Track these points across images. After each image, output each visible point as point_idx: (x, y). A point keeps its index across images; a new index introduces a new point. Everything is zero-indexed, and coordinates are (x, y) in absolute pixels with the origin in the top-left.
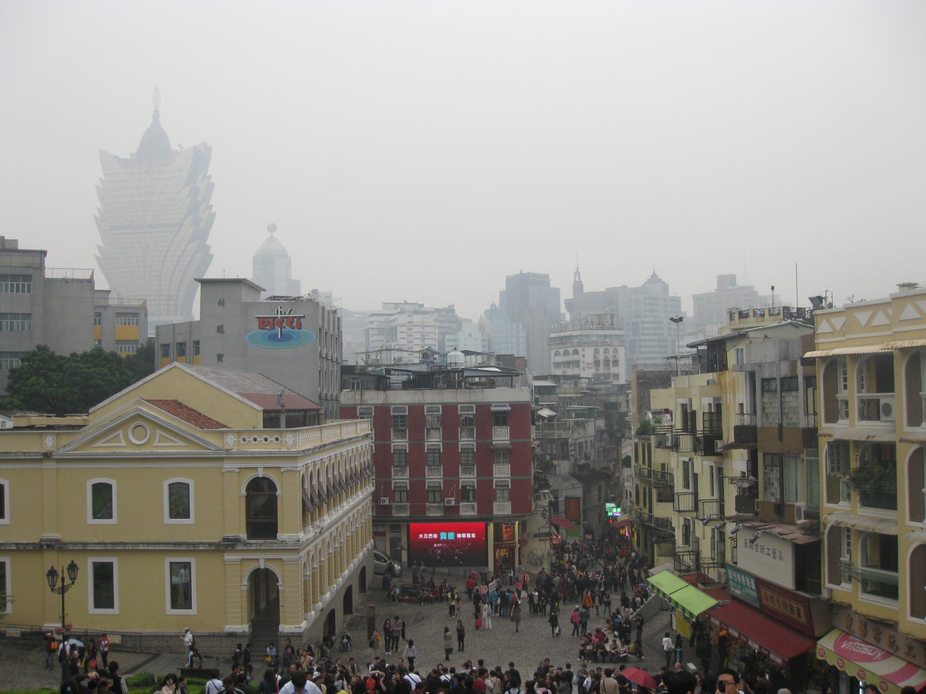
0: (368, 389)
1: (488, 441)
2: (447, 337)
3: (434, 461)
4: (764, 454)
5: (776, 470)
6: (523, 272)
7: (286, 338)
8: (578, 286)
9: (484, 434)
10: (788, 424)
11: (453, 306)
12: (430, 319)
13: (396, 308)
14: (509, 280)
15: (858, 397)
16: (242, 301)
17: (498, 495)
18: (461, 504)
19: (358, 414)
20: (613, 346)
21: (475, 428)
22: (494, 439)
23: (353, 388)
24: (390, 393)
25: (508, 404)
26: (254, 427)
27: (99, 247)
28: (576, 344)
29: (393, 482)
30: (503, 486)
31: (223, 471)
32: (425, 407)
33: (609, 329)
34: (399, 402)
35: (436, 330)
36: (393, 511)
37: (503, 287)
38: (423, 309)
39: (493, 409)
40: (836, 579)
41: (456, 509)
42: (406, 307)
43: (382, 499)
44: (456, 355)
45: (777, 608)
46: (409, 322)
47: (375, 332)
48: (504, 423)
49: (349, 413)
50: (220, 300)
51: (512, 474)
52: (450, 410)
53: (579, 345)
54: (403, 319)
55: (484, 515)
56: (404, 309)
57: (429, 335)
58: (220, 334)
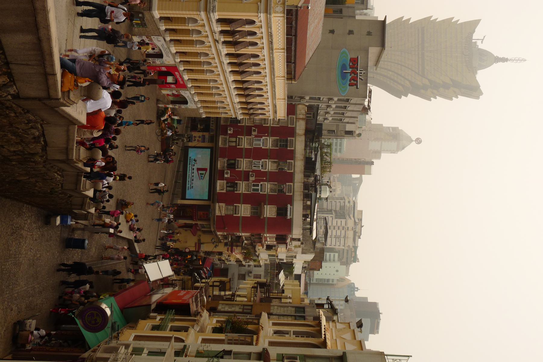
0: (307, 124)
1: (267, 203)
2: (337, 255)
5: (241, 310)
6: (381, 315)
7: (343, 76)
9: (272, 200)
11: (358, 262)
12: (350, 243)
13: (358, 219)
14: (375, 305)
15: (290, 331)
16: (370, 47)
17: (229, 207)
18: (225, 182)
21: (276, 194)
23: (308, 114)
24: (303, 138)
25: (291, 217)
26: (287, 1)
27: (409, 19)
29: (243, 137)
30: (236, 210)
34: (297, 142)
35: (342, 247)
36: (223, 136)
37: (370, 300)
38: (357, 238)
39: (289, 206)
41: (222, 178)
42: (359, 226)
43: (232, 128)
44: (327, 191)
46: (348, 228)
47: (342, 204)
48: (278, 214)
49: (291, 109)
50: (371, 33)
52: (290, 177)
54: (350, 223)
56: (358, 225)
57: (339, 241)
58: (348, 31)
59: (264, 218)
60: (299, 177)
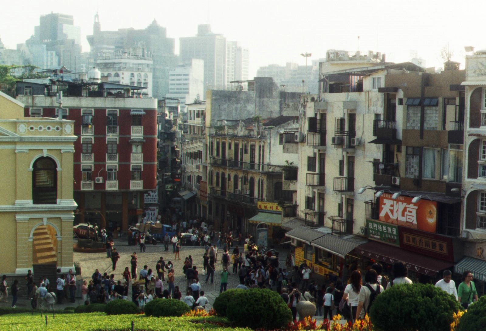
1: (128, 136)
3: (87, 150)
4: (407, 147)
8: (97, 26)
9: (125, 132)
10: (428, 128)
19: (30, 113)
20: (144, 72)
21: (118, 127)
22: (132, 135)
25: (142, 110)
28: (117, 69)
31: (16, 151)
32: (82, 110)
33: (141, 59)
37: (38, 24)
39: (132, 113)
40: (471, 224)
45: (418, 245)
48: (140, 124)
51: (144, 161)
52: (100, 112)
53: (120, 69)
55: (123, 190)
59: (144, 138)
60: (99, 103)
